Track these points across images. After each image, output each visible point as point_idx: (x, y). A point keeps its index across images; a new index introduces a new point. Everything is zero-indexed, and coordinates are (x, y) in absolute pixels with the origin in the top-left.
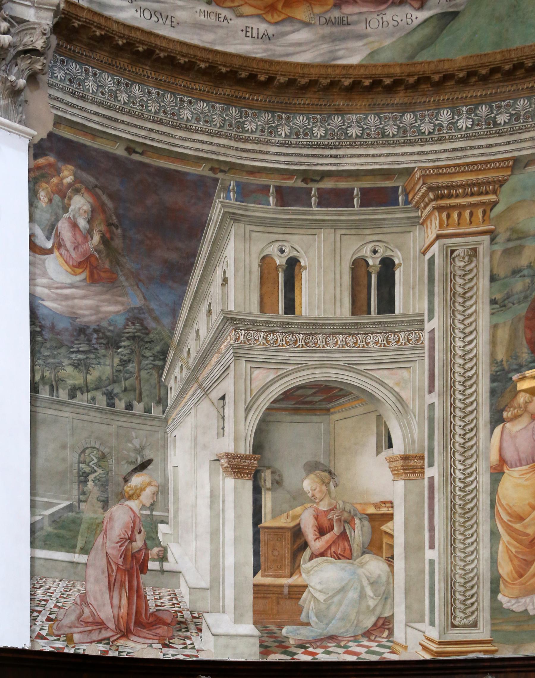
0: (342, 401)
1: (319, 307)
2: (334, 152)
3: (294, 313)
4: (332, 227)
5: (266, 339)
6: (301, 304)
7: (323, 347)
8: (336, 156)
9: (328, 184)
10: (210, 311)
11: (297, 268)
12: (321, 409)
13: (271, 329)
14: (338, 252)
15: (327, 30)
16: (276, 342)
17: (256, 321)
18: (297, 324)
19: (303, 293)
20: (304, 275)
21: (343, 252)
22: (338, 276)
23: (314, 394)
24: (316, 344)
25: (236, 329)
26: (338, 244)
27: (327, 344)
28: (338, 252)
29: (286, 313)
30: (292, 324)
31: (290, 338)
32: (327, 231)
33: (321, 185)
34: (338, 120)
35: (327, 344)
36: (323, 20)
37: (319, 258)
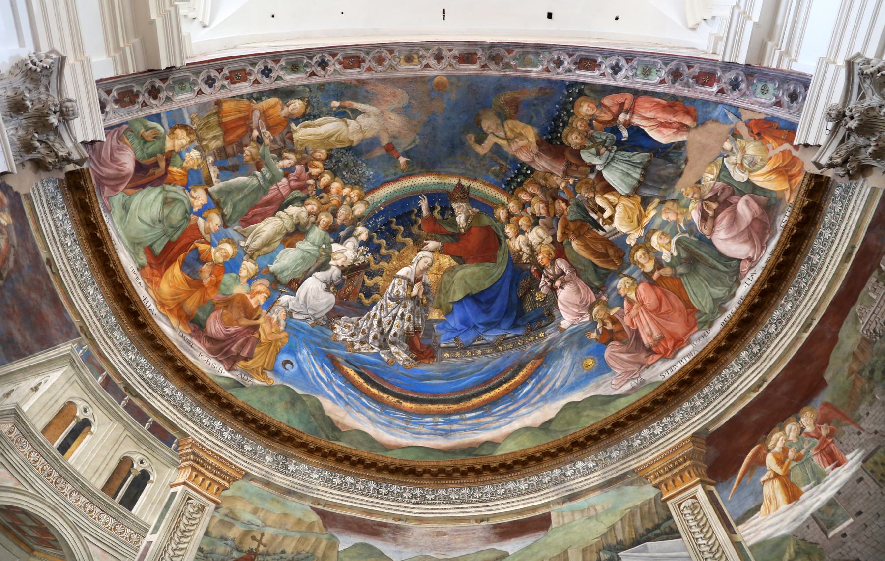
0: (49, 550)
1: (83, 466)
2: (150, 390)
3: (63, 454)
4: (125, 426)
5: (30, 453)
6: (73, 453)
7: (66, 495)
8: (151, 394)
9: (137, 402)
10: (8, 395)
11: (86, 429)
12: (27, 545)
13: (40, 450)
14: (119, 443)
15: (181, 339)
16: (36, 462)
17: (33, 435)
18: (59, 463)
19: (79, 448)
20: (88, 437)
21: (122, 445)
22: (109, 457)
23: (31, 527)
24: (63, 489)
25: (14, 425)
26: (122, 439)
27: (70, 496)
28: (119, 443)
29: (58, 449)
30: (57, 460)
31: (47, 468)
32: (121, 426)
33: (133, 399)
34: (162, 379)
35: (70, 496)
36: (181, 334)
37: (105, 436)
